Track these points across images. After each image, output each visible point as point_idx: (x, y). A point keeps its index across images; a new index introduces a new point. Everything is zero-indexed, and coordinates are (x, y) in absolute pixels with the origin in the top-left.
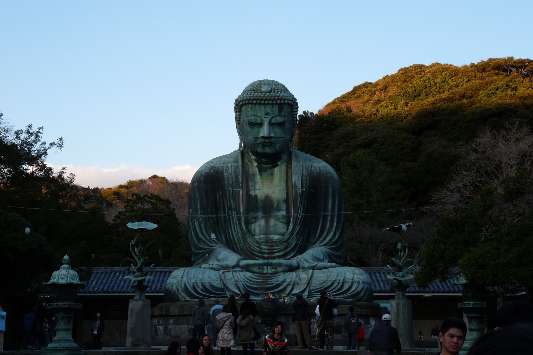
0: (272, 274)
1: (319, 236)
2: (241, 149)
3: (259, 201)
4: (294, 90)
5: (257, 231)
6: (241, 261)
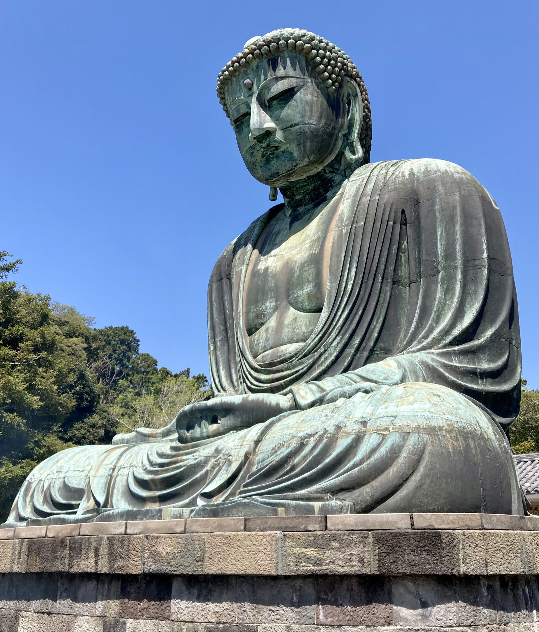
0: (209, 437)
5: (262, 344)
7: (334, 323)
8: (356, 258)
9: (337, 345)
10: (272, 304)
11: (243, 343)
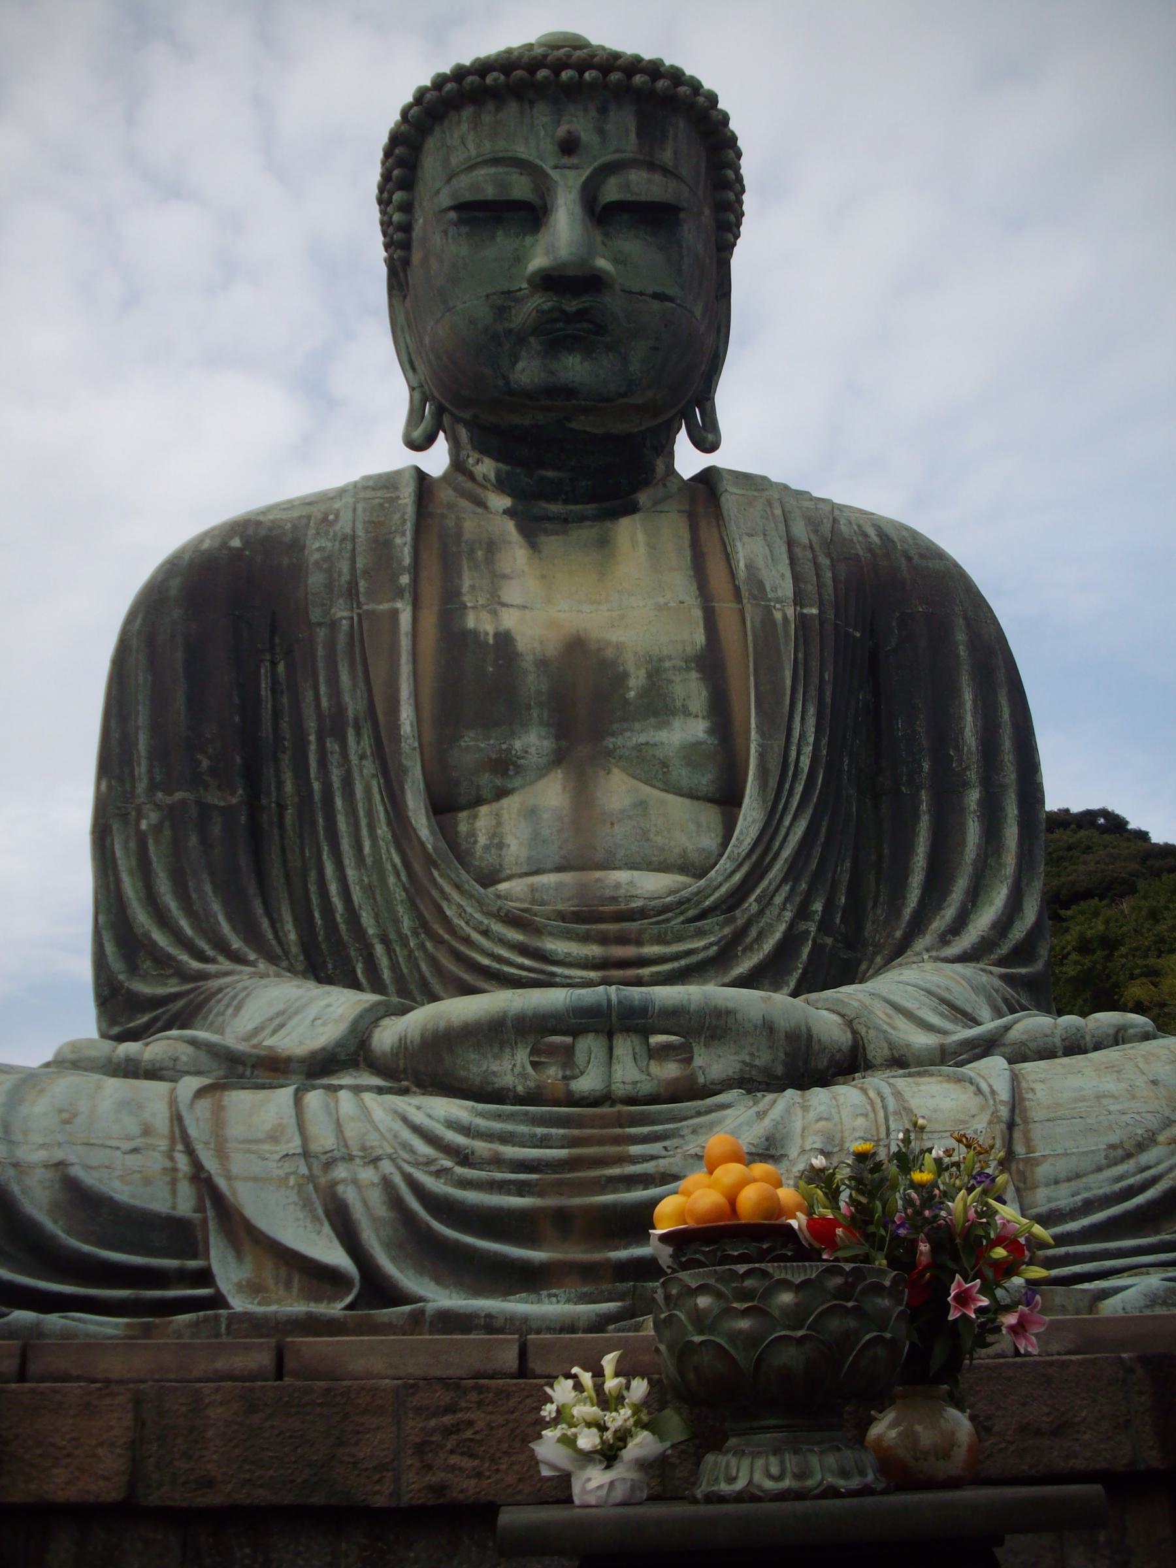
0: (653, 1099)
1: (921, 902)
2: (417, 434)
3: (528, 663)
4: (720, 99)
5: (516, 848)
6: (386, 1022)
7: (777, 844)
8: (813, 692)
9: (784, 904)
10: (546, 743)
11: (432, 832)
